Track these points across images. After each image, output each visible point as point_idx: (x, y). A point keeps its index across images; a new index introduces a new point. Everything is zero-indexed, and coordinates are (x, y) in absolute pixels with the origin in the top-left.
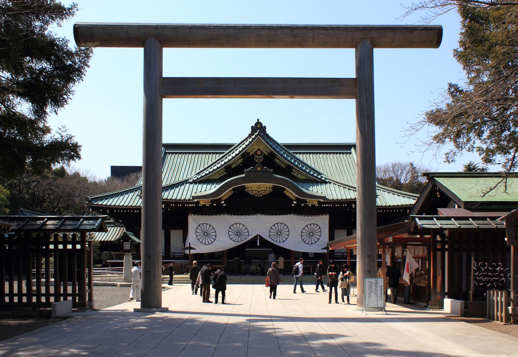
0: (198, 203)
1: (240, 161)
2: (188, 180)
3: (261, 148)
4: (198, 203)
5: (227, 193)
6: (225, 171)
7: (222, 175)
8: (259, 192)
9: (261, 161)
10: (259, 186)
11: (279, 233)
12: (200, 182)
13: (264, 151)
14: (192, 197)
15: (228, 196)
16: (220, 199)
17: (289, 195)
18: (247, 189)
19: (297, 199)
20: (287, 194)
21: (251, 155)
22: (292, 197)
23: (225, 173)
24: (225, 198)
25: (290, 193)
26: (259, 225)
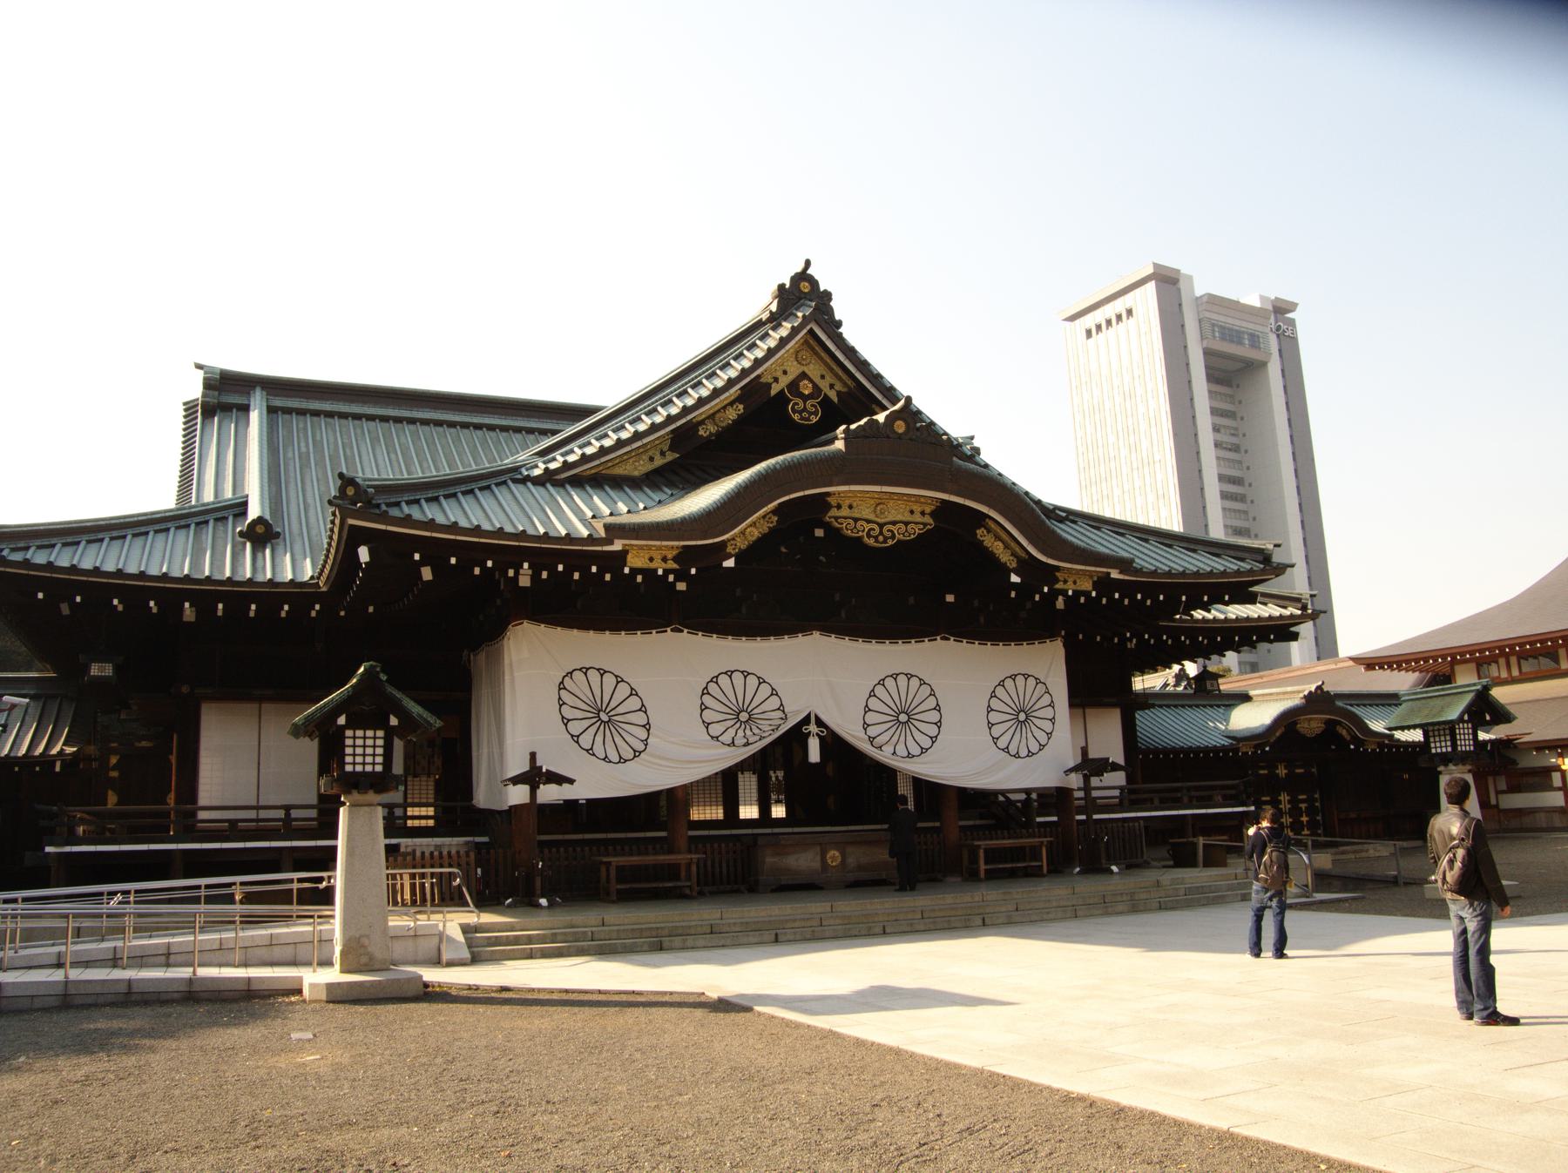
0: (622, 556)
1: (732, 414)
2: (516, 469)
3: (814, 370)
4: (622, 556)
5: (754, 524)
6: (671, 449)
7: (659, 462)
8: (881, 526)
9: (814, 419)
10: (880, 501)
11: (904, 718)
12: (578, 482)
13: (824, 385)
14: (607, 527)
15: (755, 534)
16: (720, 550)
17: (998, 548)
18: (834, 512)
19: (1028, 565)
20: (988, 541)
21: (773, 392)
22: (1005, 557)
23: (671, 456)
24: (742, 544)
25: (1004, 541)
26: (827, 681)
